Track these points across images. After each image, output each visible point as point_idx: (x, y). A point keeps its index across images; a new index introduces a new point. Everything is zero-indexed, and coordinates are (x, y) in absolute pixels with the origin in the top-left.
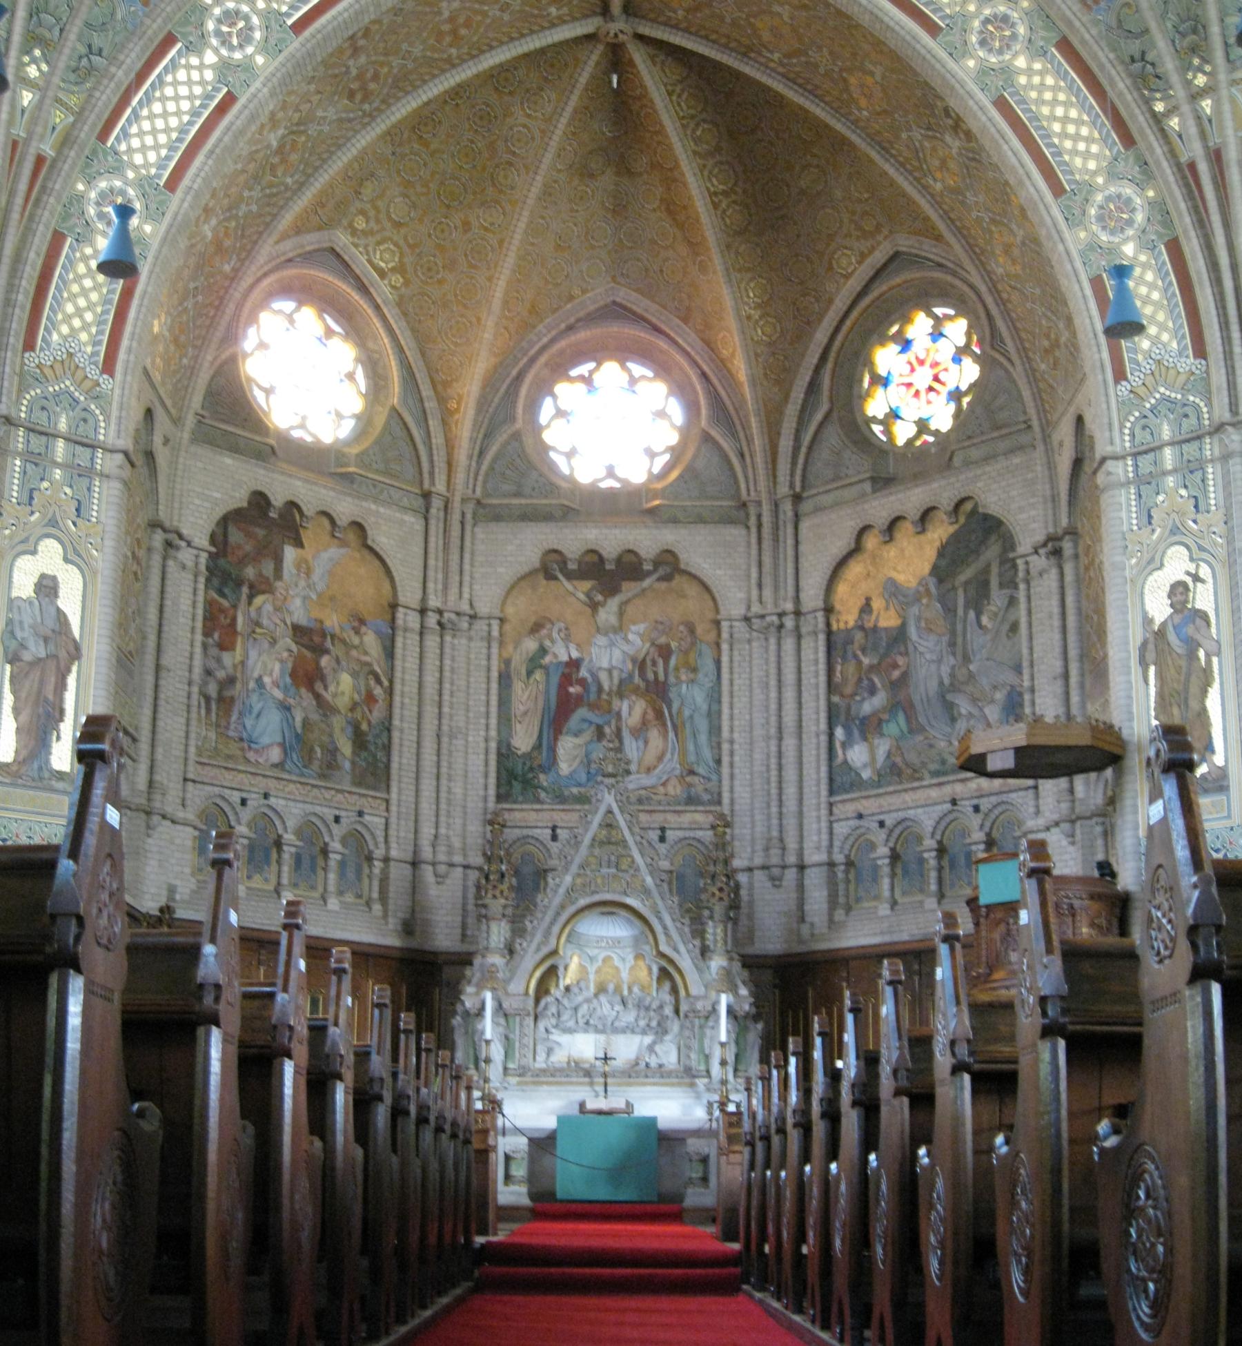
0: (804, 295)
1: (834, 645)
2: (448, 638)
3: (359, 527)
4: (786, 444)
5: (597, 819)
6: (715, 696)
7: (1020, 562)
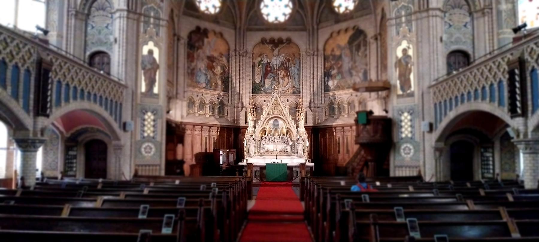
1: (326, 59)
2: (241, 58)
3: (221, 35)
4: (315, 12)
5: (274, 99)
6: (299, 70)
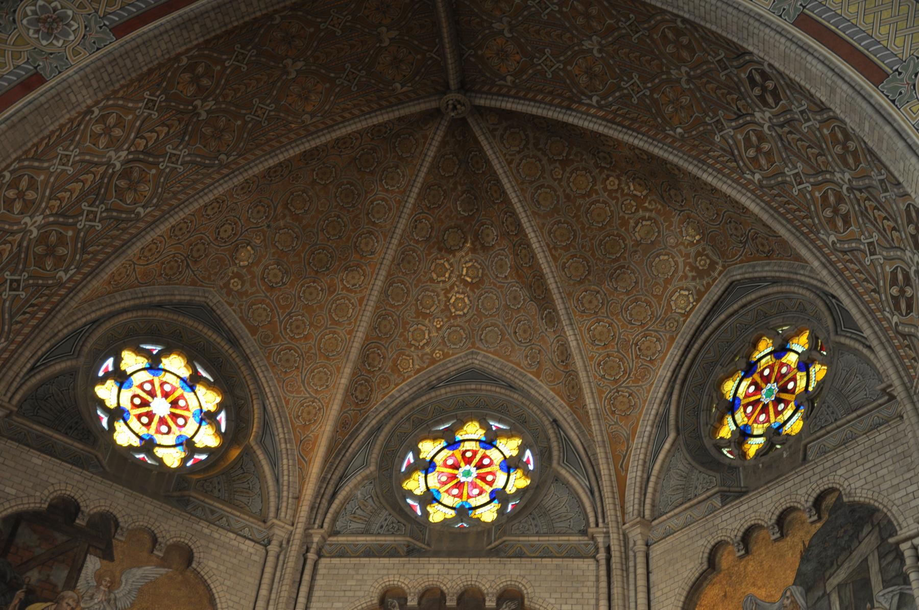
0: (645, 336)
7: (903, 546)
